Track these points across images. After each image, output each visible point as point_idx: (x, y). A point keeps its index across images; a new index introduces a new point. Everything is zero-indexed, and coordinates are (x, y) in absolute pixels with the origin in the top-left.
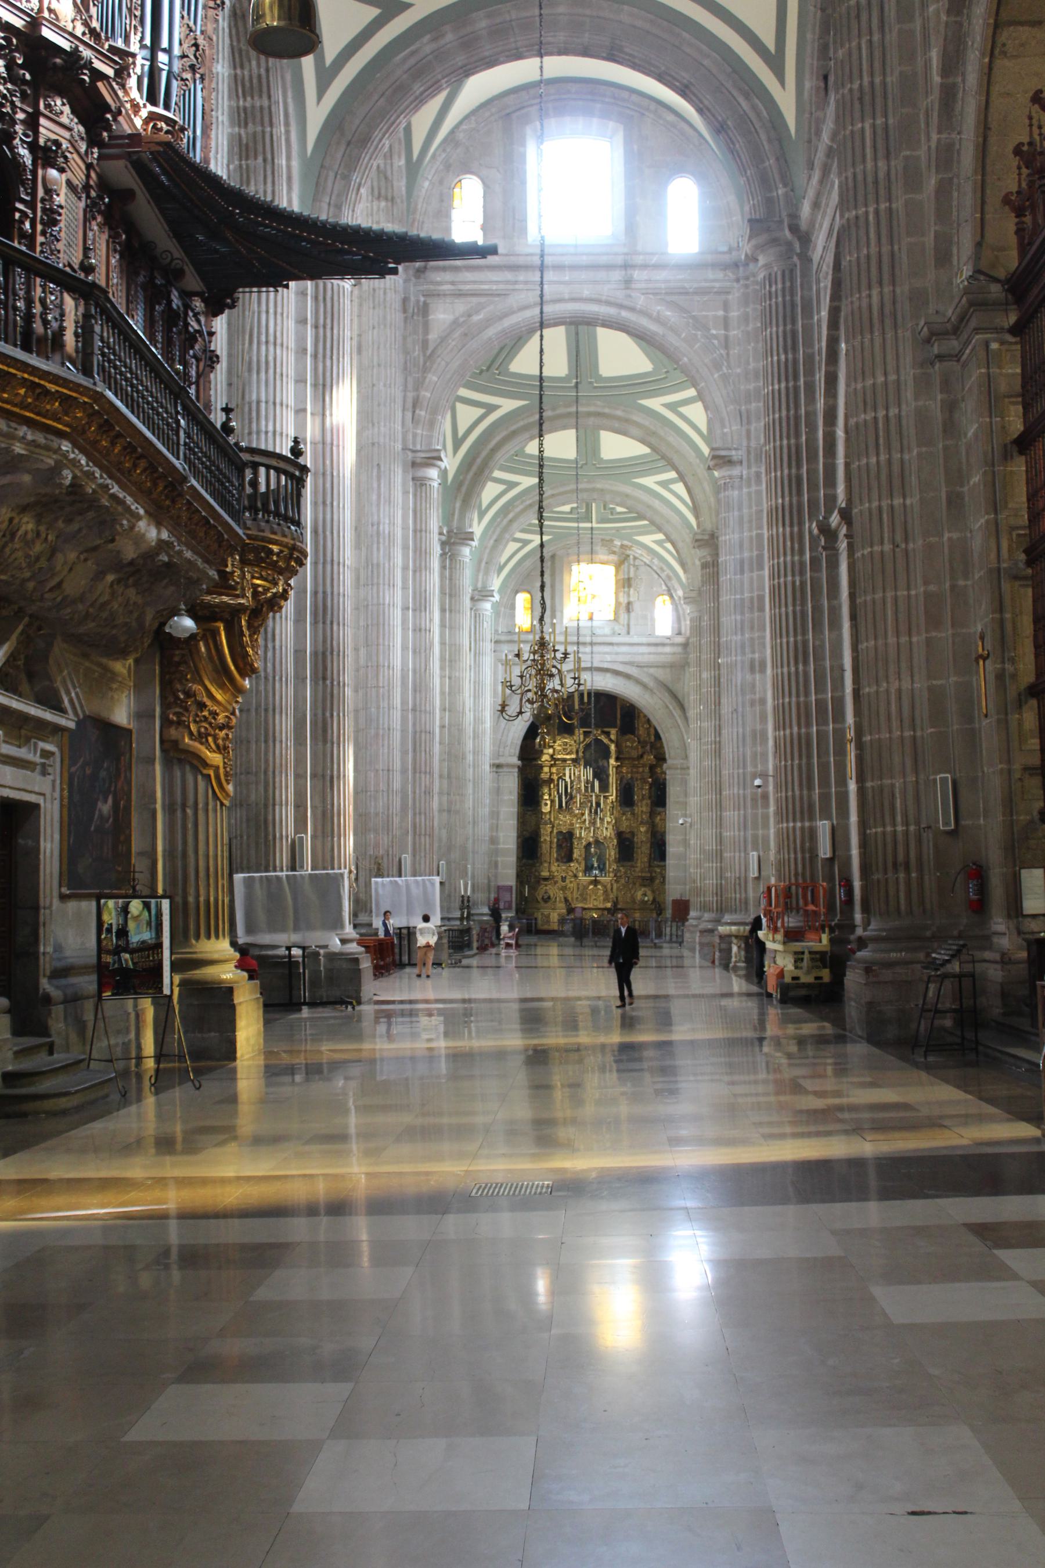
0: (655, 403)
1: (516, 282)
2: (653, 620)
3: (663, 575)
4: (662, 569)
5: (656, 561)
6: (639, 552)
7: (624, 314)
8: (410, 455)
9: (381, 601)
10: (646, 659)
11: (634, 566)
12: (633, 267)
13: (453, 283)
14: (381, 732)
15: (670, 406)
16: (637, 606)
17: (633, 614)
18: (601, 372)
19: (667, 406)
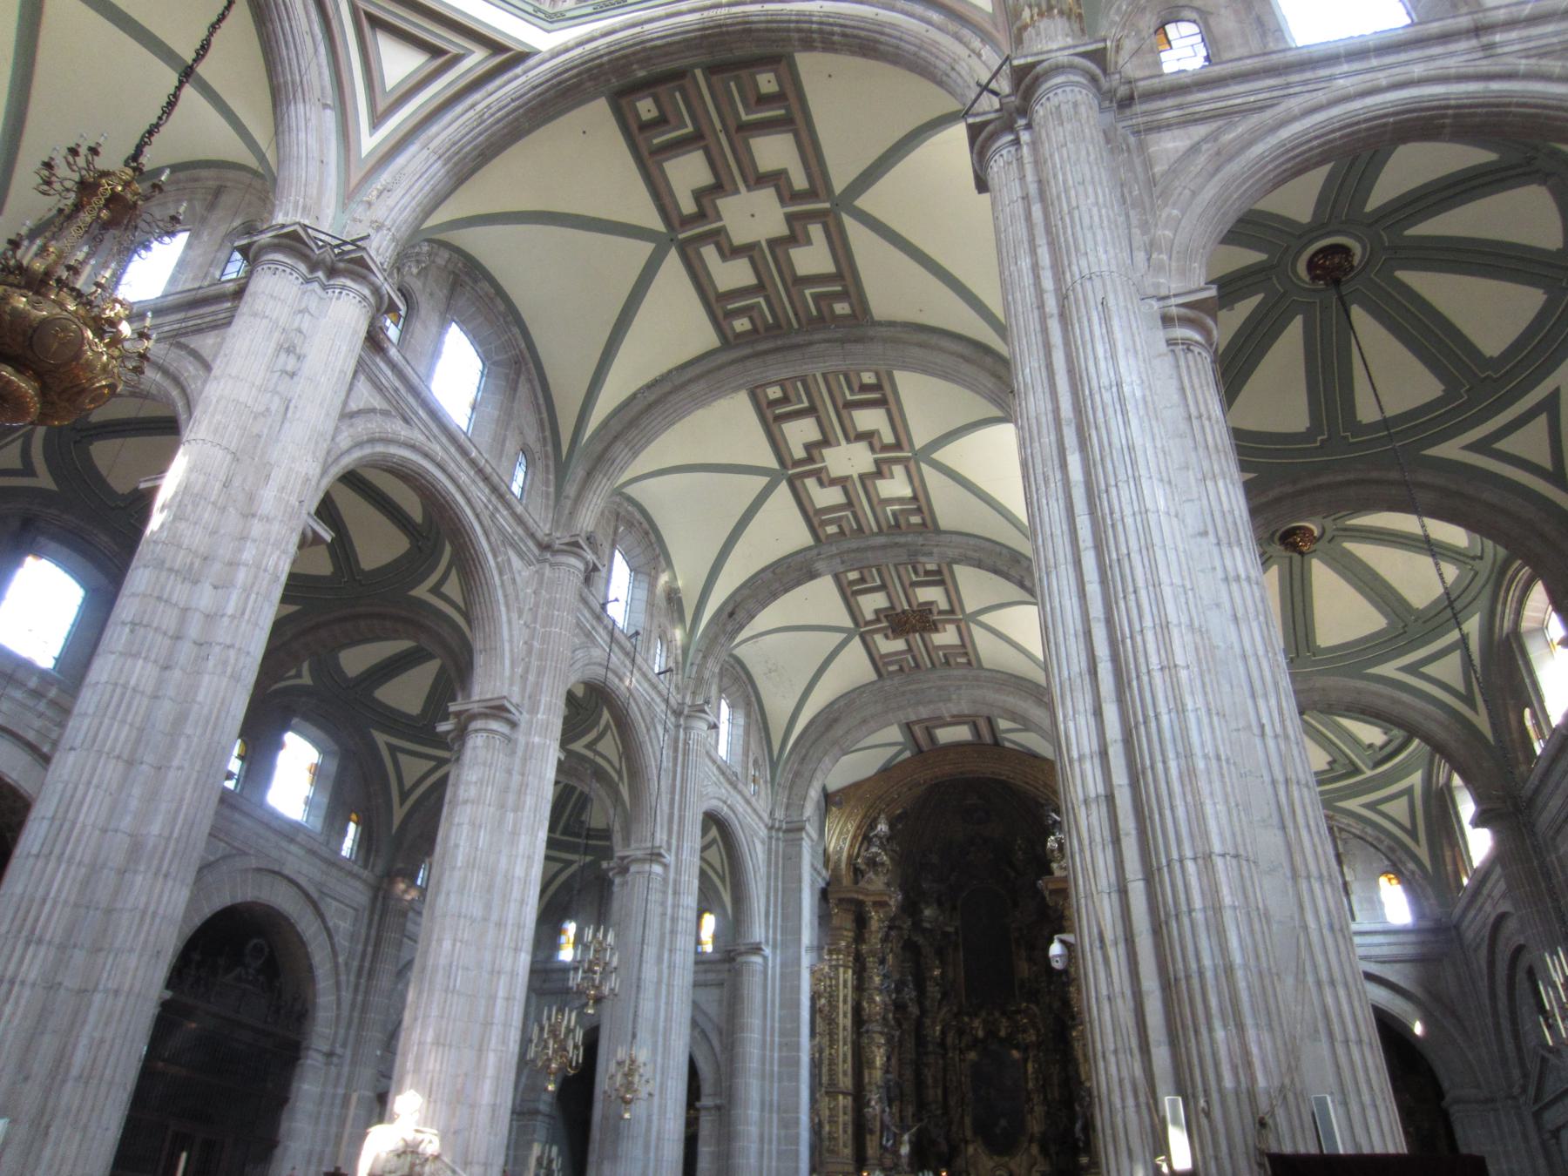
0: (1451, 450)
1: (1288, 86)
2: (1381, 903)
3: (1382, 847)
4: (1378, 839)
5: (1369, 830)
6: (1345, 821)
7: (1495, 86)
8: (1156, 305)
9: (1150, 505)
10: (1385, 951)
11: (1342, 839)
12: (1490, 28)
13: (1179, 107)
14: (1201, 764)
15: (1480, 447)
16: (1355, 888)
17: (1354, 898)
18: (1359, 418)
19: (1472, 447)
